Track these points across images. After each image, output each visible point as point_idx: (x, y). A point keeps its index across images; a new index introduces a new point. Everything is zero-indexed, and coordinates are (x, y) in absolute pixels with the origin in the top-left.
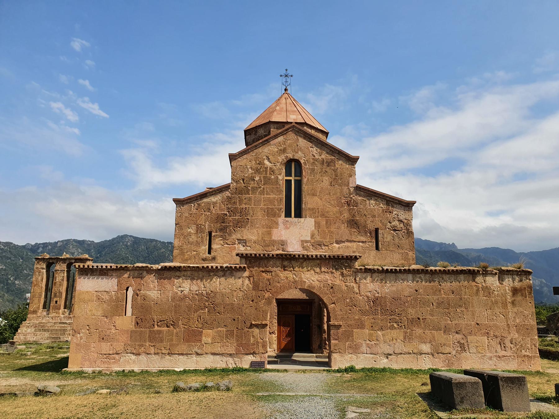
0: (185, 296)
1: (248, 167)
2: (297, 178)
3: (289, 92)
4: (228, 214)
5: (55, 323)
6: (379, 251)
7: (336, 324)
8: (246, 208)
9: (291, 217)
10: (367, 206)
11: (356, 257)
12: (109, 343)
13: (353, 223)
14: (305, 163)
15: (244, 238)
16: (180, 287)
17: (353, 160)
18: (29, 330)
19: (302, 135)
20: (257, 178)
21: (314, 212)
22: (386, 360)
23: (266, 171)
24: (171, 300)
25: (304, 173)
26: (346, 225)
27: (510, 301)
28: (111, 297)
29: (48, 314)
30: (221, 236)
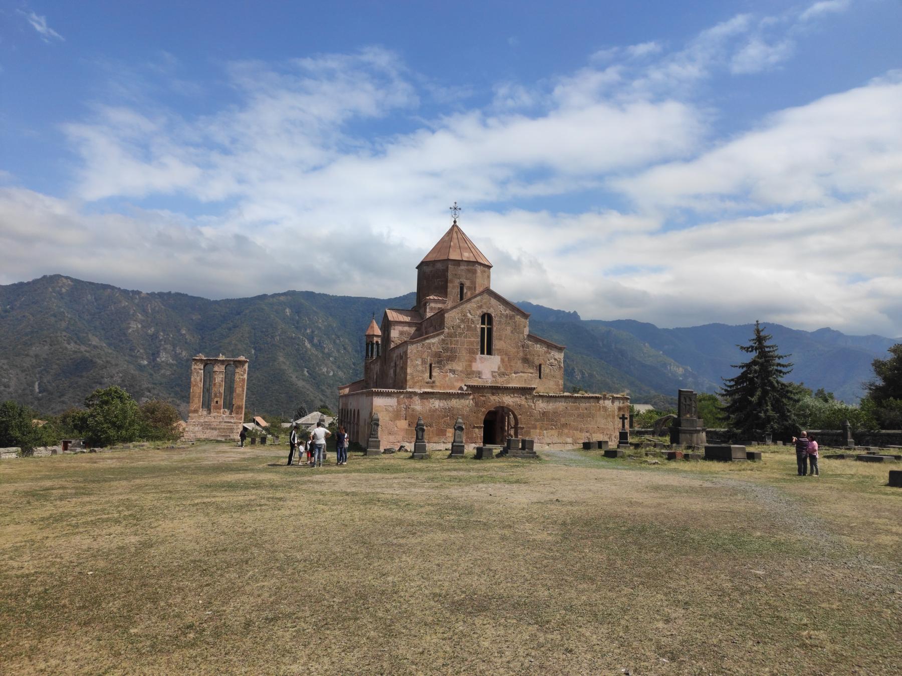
0: (436, 409)
2: (489, 326)
3: (457, 224)
5: (220, 422)
9: (484, 354)
11: (534, 388)
13: (526, 360)
14: (495, 317)
18: (197, 429)
20: (462, 326)
21: (500, 352)
22: (547, 447)
23: (468, 321)
25: (494, 324)
28: (394, 410)
29: (210, 413)
30: (438, 367)
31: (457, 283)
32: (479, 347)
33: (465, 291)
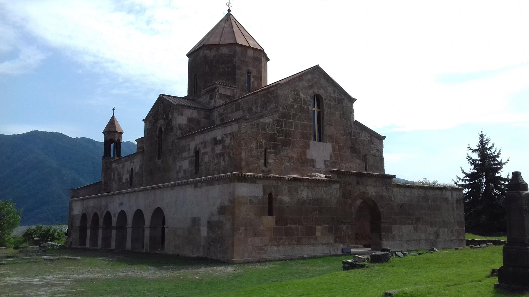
1: (290, 96)
2: (318, 110)
3: (231, 12)
4: (277, 134)
6: (367, 171)
7: (385, 222)
8: (289, 131)
10: (360, 137)
12: (260, 238)
13: (354, 150)
14: (325, 99)
15: (289, 155)
16: (301, 194)
17: (352, 100)
19: (323, 76)
20: (295, 107)
23: (301, 102)
24: (297, 204)
25: (325, 107)
26: (349, 150)
27: (455, 207)
31: (244, 71)
32: (312, 132)
33: (252, 80)
